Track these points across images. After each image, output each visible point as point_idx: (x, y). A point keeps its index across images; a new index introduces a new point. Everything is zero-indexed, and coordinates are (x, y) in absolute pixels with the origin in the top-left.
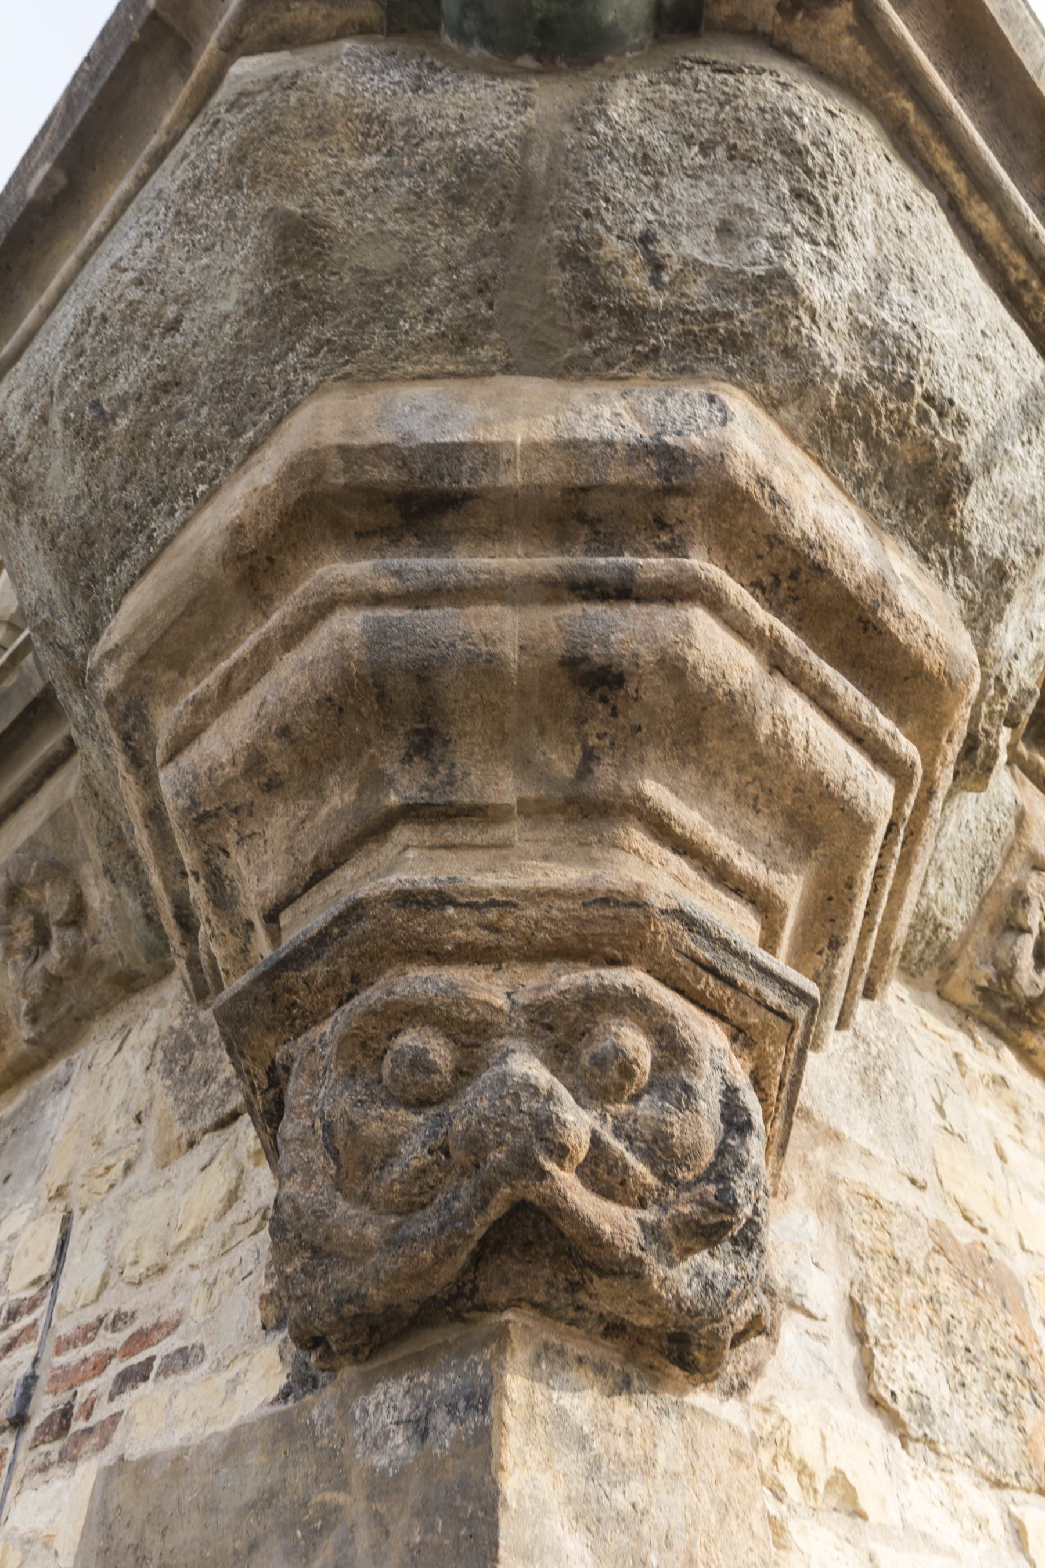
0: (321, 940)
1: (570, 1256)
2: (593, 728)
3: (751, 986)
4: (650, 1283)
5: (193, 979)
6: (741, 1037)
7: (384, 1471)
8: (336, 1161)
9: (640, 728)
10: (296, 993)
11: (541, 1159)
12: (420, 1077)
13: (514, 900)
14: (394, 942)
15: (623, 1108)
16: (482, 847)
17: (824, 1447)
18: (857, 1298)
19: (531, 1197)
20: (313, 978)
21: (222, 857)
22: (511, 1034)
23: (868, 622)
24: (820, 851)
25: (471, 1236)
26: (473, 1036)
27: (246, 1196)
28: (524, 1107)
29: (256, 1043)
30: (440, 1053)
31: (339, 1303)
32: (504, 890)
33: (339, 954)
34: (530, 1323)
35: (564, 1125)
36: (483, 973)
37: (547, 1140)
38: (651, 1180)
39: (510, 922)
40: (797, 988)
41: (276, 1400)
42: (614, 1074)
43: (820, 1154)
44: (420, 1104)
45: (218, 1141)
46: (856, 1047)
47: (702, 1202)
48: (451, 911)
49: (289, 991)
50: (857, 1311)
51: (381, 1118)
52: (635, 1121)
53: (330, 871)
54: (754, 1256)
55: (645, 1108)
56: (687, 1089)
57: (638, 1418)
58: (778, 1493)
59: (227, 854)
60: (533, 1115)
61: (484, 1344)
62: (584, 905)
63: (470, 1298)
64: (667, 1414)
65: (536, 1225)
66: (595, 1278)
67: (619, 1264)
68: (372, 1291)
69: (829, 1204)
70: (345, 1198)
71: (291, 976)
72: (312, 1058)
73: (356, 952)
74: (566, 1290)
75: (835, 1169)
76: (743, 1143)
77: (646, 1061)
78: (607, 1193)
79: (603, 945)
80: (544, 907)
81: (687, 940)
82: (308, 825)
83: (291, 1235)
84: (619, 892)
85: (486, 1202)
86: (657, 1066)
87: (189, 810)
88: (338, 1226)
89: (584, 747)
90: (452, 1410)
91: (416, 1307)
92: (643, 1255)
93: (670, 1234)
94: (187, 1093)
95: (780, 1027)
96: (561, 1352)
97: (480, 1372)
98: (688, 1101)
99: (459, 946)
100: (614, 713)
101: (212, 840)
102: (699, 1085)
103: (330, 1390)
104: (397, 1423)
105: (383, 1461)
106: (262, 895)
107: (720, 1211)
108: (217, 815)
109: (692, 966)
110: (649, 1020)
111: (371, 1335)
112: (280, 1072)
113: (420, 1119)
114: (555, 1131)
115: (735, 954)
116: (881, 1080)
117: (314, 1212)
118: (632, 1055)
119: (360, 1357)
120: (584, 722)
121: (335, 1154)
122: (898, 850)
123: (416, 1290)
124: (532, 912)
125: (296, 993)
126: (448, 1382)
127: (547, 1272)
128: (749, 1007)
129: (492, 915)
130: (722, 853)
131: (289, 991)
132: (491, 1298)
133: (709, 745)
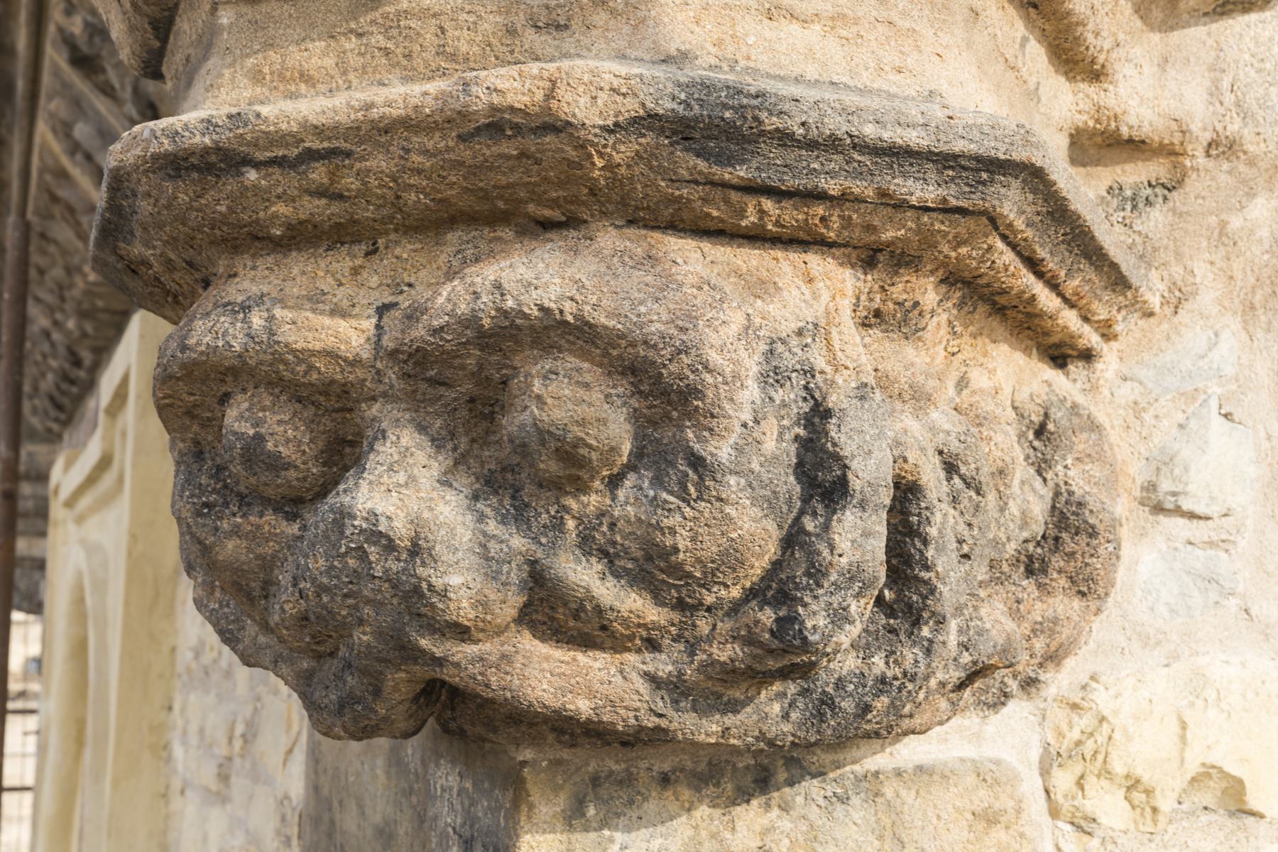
11: (424, 643)
15: (593, 501)
17: (1183, 739)
22: (384, 394)
34: (566, 754)
35: (444, 594)
38: (654, 614)
40: (978, 158)
47: (750, 640)
48: (252, 175)
51: (236, 532)
52: (612, 525)
54: (925, 632)
55: (628, 504)
56: (697, 462)
57: (785, 824)
58: (1084, 825)
62: (462, 138)
64: (844, 800)
76: (826, 527)
84: (512, 109)
86: (643, 424)
96: (627, 781)
98: (700, 485)
99: (290, 227)
102: (721, 451)
109: (719, 191)
110: (606, 354)
113: (294, 529)
114: (432, 606)
115: (812, 145)
124: (379, 162)
129: (318, 174)
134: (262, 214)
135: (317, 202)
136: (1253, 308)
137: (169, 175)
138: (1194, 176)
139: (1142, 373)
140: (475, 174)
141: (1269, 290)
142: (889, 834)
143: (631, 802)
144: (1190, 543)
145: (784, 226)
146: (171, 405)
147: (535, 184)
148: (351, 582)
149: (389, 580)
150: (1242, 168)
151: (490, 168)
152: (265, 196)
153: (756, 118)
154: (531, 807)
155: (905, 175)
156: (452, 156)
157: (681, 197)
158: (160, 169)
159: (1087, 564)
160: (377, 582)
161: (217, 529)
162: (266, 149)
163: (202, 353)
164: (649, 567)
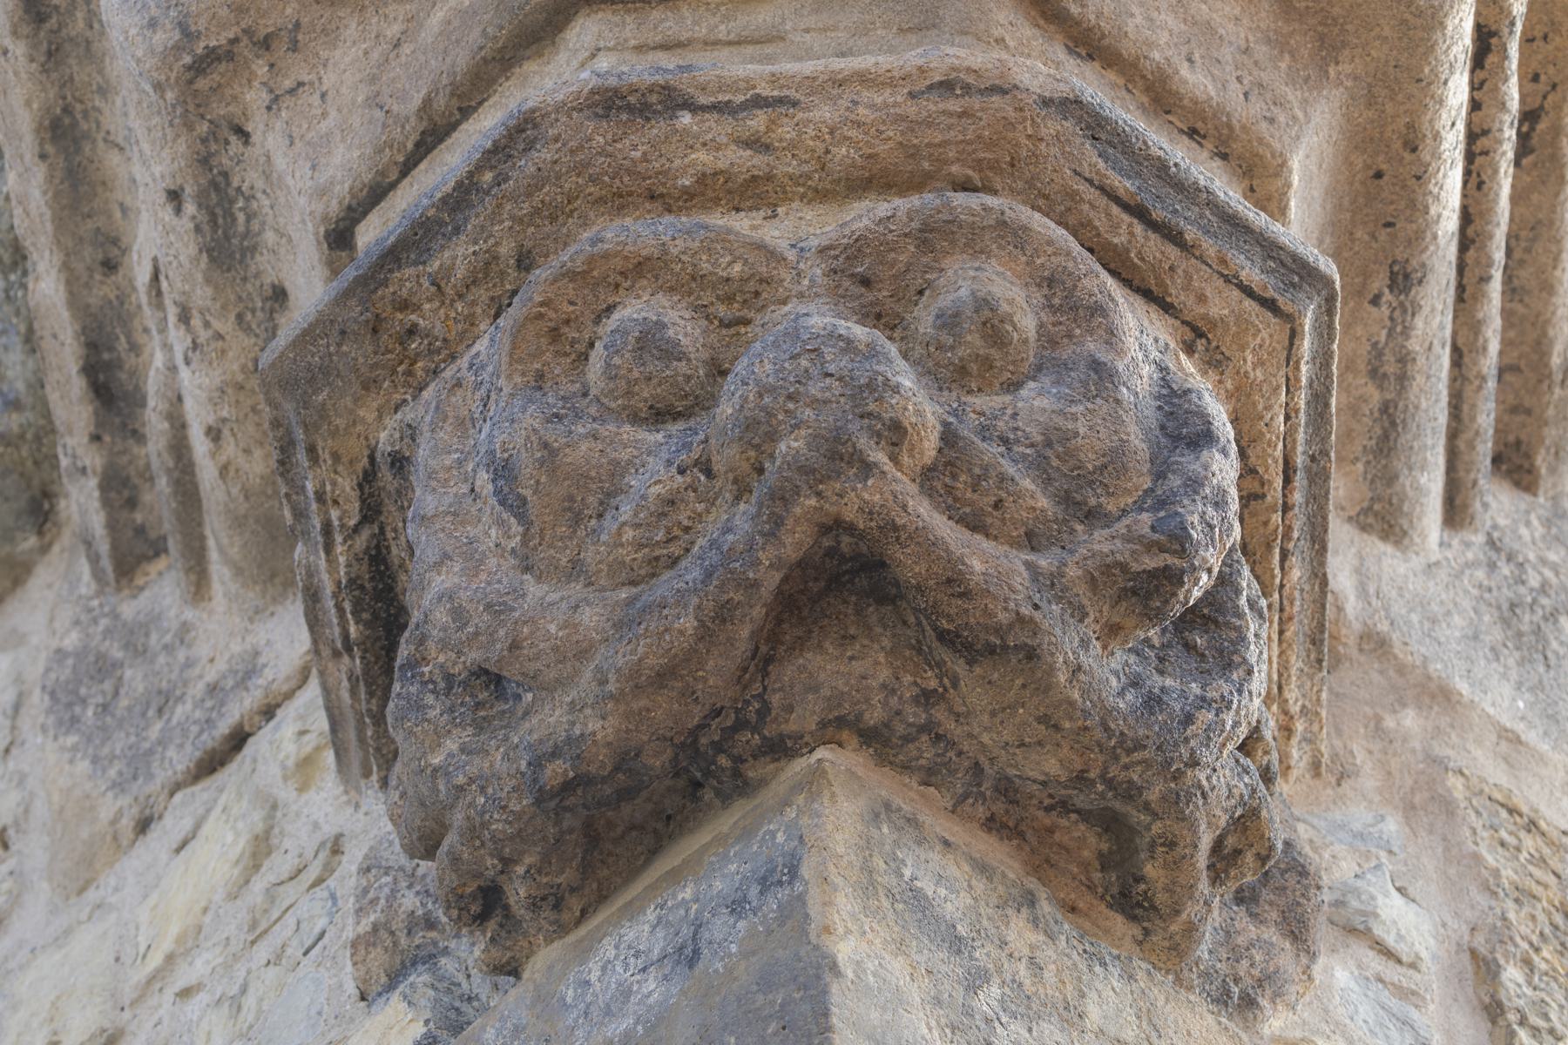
0: (462, 197)
1: (919, 651)
3: (1209, 247)
4: (1051, 670)
5: (112, 526)
6: (1200, 344)
7: (628, 1035)
8: (521, 517)
10: (417, 308)
13: (792, 93)
14: (594, 180)
16: (730, 43)
18: (1483, 950)
19: (849, 514)
20: (447, 271)
21: (235, 142)
22: (801, 295)
24: (1346, 68)
25: (755, 584)
26: (737, 301)
27: (288, 843)
28: (832, 368)
29: (340, 422)
30: (683, 326)
31: (537, 764)
32: (774, 79)
33: (494, 217)
36: (746, 223)
37: (870, 415)
39: (786, 131)
40: (1295, 257)
42: (974, 339)
43: (1409, 720)
44: (659, 415)
45: (205, 796)
46: (1492, 566)
48: (686, 119)
49: (404, 306)
50: (1485, 968)
53: (453, 127)
59: (243, 134)
61: (787, 803)
62: (912, 95)
63: (755, 730)
64: (1104, 965)
65: (858, 613)
66: (960, 667)
67: (998, 630)
68: (594, 725)
69: (1427, 799)
70: (539, 579)
71: (406, 279)
73: (526, 208)
74: (916, 700)
75: (1440, 750)
77: (1028, 323)
78: (975, 525)
79: (946, 162)
80: (844, 103)
81: (1091, 158)
82: (406, 49)
83: (432, 714)
84: (969, 70)
85: (778, 522)
86: (1049, 340)
87: (177, 48)
88: (531, 621)
90: (737, 906)
91: (669, 753)
92: (1037, 615)
93: (1081, 589)
94: (119, 742)
95: (1268, 330)
96: (912, 821)
99: (702, 179)
101: (219, 110)
103: (513, 992)
104: (644, 970)
105: (626, 1023)
106: (322, 192)
107: (1162, 550)
108: (230, 56)
109: (1103, 201)
111: (586, 869)
112: (386, 476)
113: (660, 437)
116: (1547, 628)
117: (488, 606)
118: (1005, 307)
119: (566, 917)
121: (519, 508)
122: (1512, 91)
123: (664, 709)
124: (824, 113)
125: (417, 308)
127: (884, 674)
128: (1213, 287)
129: (757, 121)
130: (1156, 55)
131: (404, 306)
132: (792, 727)
134: (678, 162)
136: (1413, 807)
137: (597, 115)
138: (1347, 664)
139: (1315, 822)
140: (913, 131)
141: (1426, 795)
142: (1144, 1018)
143: (919, 844)
144: (1381, 980)
145: (1142, 259)
146: (540, 316)
147: (969, 143)
148: (799, 382)
149: (840, 379)
150: (1391, 673)
151: (929, 125)
152: (689, 142)
153: (1145, 143)
154: (833, 795)
155: (1239, 248)
156: (898, 110)
157: (1077, 192)
158: (589, 107)
159: (1298, 904)
160: (828, 380)
161: (571, 432)
162: (713, 93)
163: (618, 244)
164: (1049, 453)
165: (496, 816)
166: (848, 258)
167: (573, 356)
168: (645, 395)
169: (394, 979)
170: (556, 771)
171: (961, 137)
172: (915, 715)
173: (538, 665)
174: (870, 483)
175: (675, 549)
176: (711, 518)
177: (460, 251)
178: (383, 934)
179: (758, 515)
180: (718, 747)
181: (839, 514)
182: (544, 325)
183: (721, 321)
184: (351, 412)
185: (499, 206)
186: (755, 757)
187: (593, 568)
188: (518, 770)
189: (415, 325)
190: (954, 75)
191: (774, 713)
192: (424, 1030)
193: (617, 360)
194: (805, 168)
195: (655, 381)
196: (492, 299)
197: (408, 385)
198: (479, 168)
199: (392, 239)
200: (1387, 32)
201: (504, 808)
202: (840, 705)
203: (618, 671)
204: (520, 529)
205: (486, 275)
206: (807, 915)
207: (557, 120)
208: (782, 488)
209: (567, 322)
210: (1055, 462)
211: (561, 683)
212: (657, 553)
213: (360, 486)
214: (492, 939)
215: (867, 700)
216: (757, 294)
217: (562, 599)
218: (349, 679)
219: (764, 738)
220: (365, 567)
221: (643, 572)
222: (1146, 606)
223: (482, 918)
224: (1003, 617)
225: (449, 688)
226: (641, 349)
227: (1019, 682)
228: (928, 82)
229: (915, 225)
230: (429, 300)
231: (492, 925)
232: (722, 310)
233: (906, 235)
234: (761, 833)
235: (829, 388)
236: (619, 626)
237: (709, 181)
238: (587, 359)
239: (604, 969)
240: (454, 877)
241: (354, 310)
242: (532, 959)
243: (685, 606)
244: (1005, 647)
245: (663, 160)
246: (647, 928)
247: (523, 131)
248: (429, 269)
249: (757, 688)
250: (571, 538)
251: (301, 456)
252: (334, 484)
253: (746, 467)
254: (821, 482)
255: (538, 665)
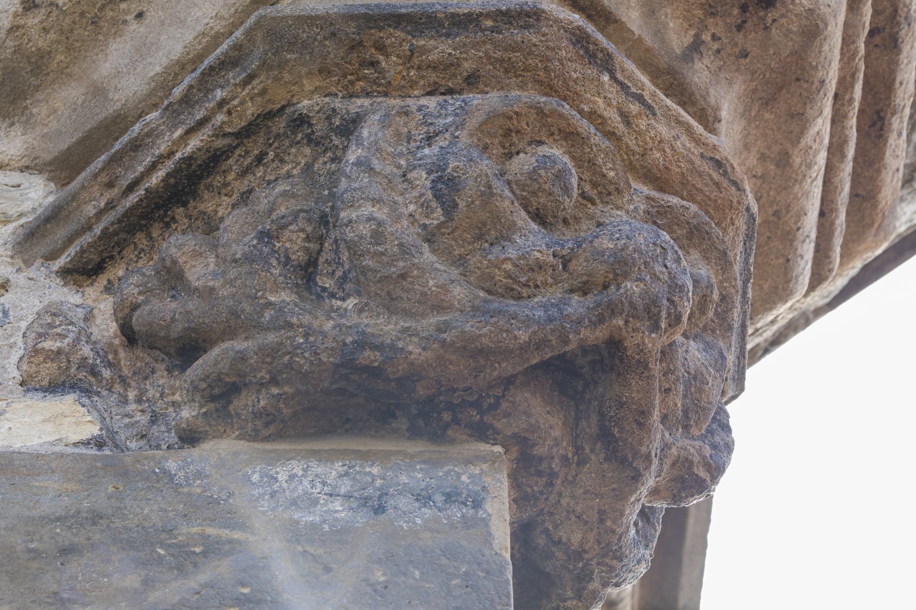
2: (716, 26)
9: (746, 56)
10: (387, 55)
12: (557, 190)
13: (656, 107)
14: (546, 69)
23: (882, 119)
25: (566, 342)
28: (668, 264)
29: (287, 77)
33: (475, 45)
39: (643, 123)
41: (86, 443)
48: (606, 78)
49: (381, 48)
60: (672, 277)
61: (468, 462)
62: (702, 156)
63: (481, 413)
67: (636, 453)
70: (434, 251)
71: (394, 36)
72: (401, 120)
73: (498, 54)
85: (601, 320)
89: (697, 36)
90: (424, 498)
93: (668, 462)
97: (464, 478)
100: (739, 28)
112: (280, 124)
117: (401, 245)
120: (713, 14)
124: (663, 130)
125: (387, 55)
126: (415, 477)
129: (634, 108)
131: (381, 48)
132: (498, 425)
133: (767, 116)
134: (588, 95)
135: (616, 116)
137: (571, 40)
146: (510, 118)
147: (710, 200)
149: (670, 273)
158: (571, 33)
160: (664, 269)
162: (624, 77)
164: (693, 383)
165: (306, 355)
166: (658, 212)
167: (506, 151)
168: (541, 201)
169: (54, 388)
170: (369, 356)
171: (708, 193)
172: (557, 465)
173: (404, 295)
174: (653, 335)
175: (525, 292)
176: (551, 290)
177: (441, 47)
178: (63, 358)
179: (593, 309)
180: (451, 407)
181: (625, 339)
182: (509, 124)
183: (583, 192)
184: (300, 77)
185: (484, 42)
186: (466, 426)
187: (472, 268)
188: (344, 340)
189: (378, 62)
190: (725, 162)
191: (499, 411)
192: (99, 433)
193: (542, 172)
194: (637, 149)
195: (552, 198)
196: (436, 83)
197: (345, 87)
198: (488, 15)
199: (403, 11)
200: (766, 286)
201: (316, 354)
202: (533, 432)
203: (463, 332)
204: (442, 219)
205: (445, 69)
206: (489, 534)
207: (552, 26)
208: (616, 305)
209: (518, 132)
210: (693, 390)
211: (407, 314)
212: (514, 286)
213: (259, 115)
214: (205, 413)
215: (545, 440)
216: (609, 194)
217: (445, 271)
218: (107, 204)
219: (481, 420)
220: (204, 157)
221: (500, 290)
222: (679, 492)
223: (213, 398)
224: (644, 449)
225: (286, 264)
226: (557, 176)
227: (615, 486)
228: (712, 155)
229: (695, 221)
230: (398, 56)
231: (212, 406)
232: (587, 188)
233: (688, 223)
234: (446, 469)
235: (663, 273)
236: (474, 308)
237: (594, 117)
238: (510, 158)
239: (292, 477)
240: (227, 366)
241: (351, 29)
242: (216, 440)
243: (528, 326)
244: (631, 465)
245: (583, 89)
246: (334, 473)
247: (529, 17)
248: (414, 42)
249: (499, 392)
250: (469, 244)
251: (234, 76)
252: (242, 103)
253: (601, 280)
254: (633, 317)
255: (404, 295)
